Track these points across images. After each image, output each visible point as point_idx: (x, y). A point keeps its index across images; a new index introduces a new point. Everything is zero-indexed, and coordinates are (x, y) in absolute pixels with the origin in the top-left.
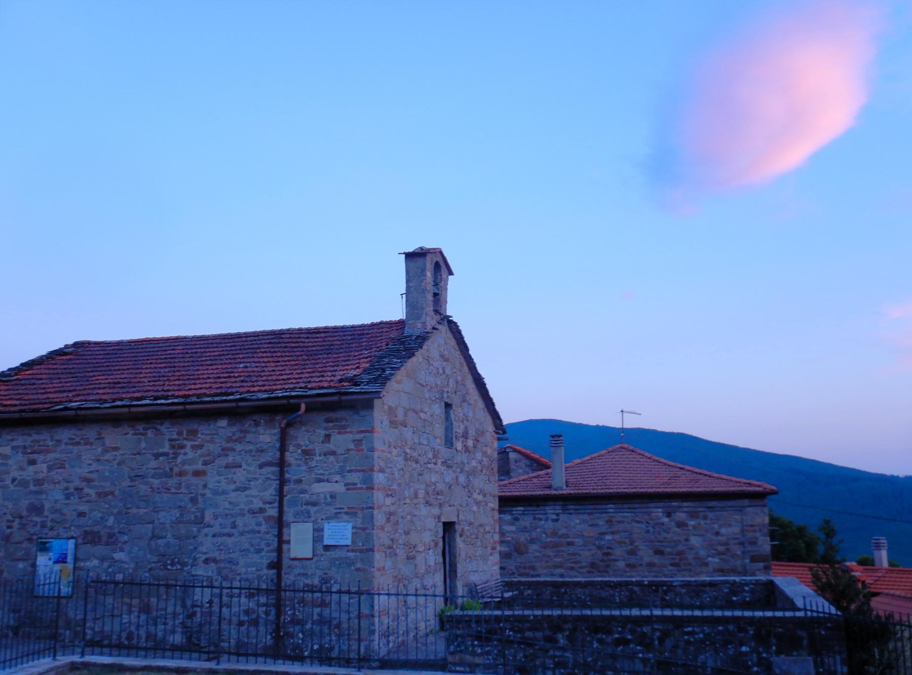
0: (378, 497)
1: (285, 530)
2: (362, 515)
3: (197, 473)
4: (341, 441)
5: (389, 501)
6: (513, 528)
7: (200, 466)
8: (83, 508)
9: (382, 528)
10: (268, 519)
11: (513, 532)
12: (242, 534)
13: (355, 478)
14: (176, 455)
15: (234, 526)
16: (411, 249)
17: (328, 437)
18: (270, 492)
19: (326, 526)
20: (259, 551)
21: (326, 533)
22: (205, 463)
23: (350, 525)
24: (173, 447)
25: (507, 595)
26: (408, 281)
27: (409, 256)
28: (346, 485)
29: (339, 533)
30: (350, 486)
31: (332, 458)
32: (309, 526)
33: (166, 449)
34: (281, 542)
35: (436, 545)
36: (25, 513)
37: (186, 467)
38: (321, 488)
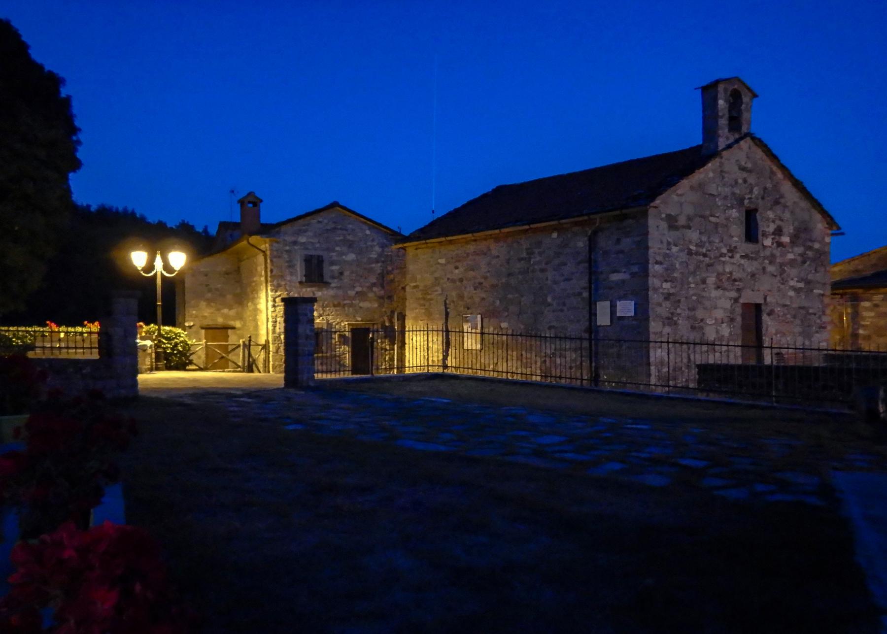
0: (653, 282)
1: (593, 306)
2: (640, 294)
3: (542, 271)
4: (627, 243)
5: (666, 285)
6: (872, 314)
7: (543, 266)
8: (483, 295)
9: (660, 305)
10: (583, 299)
11: (872, 317)
12: (568, 310)
13: (635, 269)
14: (530, 258)
15: (564, 304)
16: (704, 84)
17: (618, 241)
18: (584, 283)
19: (618, 303)
20: (578, 321)
21: (619, 308)
22: (547, 264)
23: (633, 303)
24: (528, 254)
25: (392, 276)
26: (704, 111)
27: (704, 89)
28: (631, 274)
29: (626, 308)
30: (633, 275)
31: (621, 256)
32: (608, 303)
33: (524, 255)
34: (592, 314)
35: (732, 320)
36: (455, 300)
37: (536, 267)
38: (615, 277)
